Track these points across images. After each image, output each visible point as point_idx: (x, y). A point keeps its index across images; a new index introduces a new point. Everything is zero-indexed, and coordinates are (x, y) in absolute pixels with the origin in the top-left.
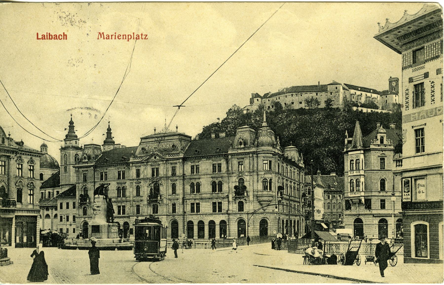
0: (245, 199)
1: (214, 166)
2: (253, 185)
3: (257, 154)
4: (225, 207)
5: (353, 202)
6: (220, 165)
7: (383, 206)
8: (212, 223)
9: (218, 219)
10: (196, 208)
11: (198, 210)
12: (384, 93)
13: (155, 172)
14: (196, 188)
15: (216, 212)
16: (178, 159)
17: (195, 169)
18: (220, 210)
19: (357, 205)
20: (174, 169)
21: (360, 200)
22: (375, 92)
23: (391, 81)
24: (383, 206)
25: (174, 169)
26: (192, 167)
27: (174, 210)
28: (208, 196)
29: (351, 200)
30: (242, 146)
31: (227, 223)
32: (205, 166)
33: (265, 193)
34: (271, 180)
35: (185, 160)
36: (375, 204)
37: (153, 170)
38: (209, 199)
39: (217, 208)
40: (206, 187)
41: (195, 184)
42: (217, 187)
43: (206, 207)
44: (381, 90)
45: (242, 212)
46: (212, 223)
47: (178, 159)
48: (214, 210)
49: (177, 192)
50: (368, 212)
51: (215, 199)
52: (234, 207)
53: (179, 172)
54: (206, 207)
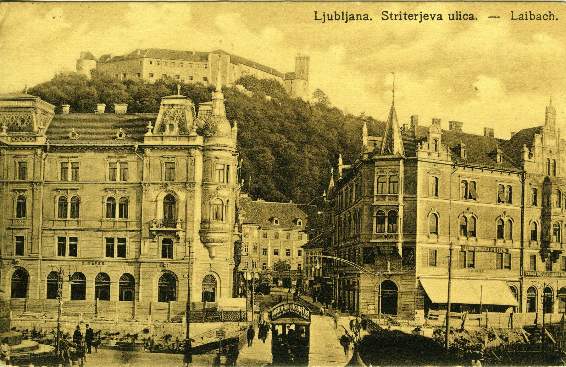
0: (177, 237)
3: (203, 150)
8: (104, 278)
9: (116, 270)
11: (73, 252)
12: (290, 77)
21: (396, 249)
22: (275, 73)
28: (97, 225)
31: (136, 281)
34: (228, 201)
38: (98, 230)
40: (94, 208)
42: (116, 208)
43: (91, 247)
44: (284, 73)
47: (34, 148)
51: (112, 233)
52: (152, 249)
54: (91, 247)
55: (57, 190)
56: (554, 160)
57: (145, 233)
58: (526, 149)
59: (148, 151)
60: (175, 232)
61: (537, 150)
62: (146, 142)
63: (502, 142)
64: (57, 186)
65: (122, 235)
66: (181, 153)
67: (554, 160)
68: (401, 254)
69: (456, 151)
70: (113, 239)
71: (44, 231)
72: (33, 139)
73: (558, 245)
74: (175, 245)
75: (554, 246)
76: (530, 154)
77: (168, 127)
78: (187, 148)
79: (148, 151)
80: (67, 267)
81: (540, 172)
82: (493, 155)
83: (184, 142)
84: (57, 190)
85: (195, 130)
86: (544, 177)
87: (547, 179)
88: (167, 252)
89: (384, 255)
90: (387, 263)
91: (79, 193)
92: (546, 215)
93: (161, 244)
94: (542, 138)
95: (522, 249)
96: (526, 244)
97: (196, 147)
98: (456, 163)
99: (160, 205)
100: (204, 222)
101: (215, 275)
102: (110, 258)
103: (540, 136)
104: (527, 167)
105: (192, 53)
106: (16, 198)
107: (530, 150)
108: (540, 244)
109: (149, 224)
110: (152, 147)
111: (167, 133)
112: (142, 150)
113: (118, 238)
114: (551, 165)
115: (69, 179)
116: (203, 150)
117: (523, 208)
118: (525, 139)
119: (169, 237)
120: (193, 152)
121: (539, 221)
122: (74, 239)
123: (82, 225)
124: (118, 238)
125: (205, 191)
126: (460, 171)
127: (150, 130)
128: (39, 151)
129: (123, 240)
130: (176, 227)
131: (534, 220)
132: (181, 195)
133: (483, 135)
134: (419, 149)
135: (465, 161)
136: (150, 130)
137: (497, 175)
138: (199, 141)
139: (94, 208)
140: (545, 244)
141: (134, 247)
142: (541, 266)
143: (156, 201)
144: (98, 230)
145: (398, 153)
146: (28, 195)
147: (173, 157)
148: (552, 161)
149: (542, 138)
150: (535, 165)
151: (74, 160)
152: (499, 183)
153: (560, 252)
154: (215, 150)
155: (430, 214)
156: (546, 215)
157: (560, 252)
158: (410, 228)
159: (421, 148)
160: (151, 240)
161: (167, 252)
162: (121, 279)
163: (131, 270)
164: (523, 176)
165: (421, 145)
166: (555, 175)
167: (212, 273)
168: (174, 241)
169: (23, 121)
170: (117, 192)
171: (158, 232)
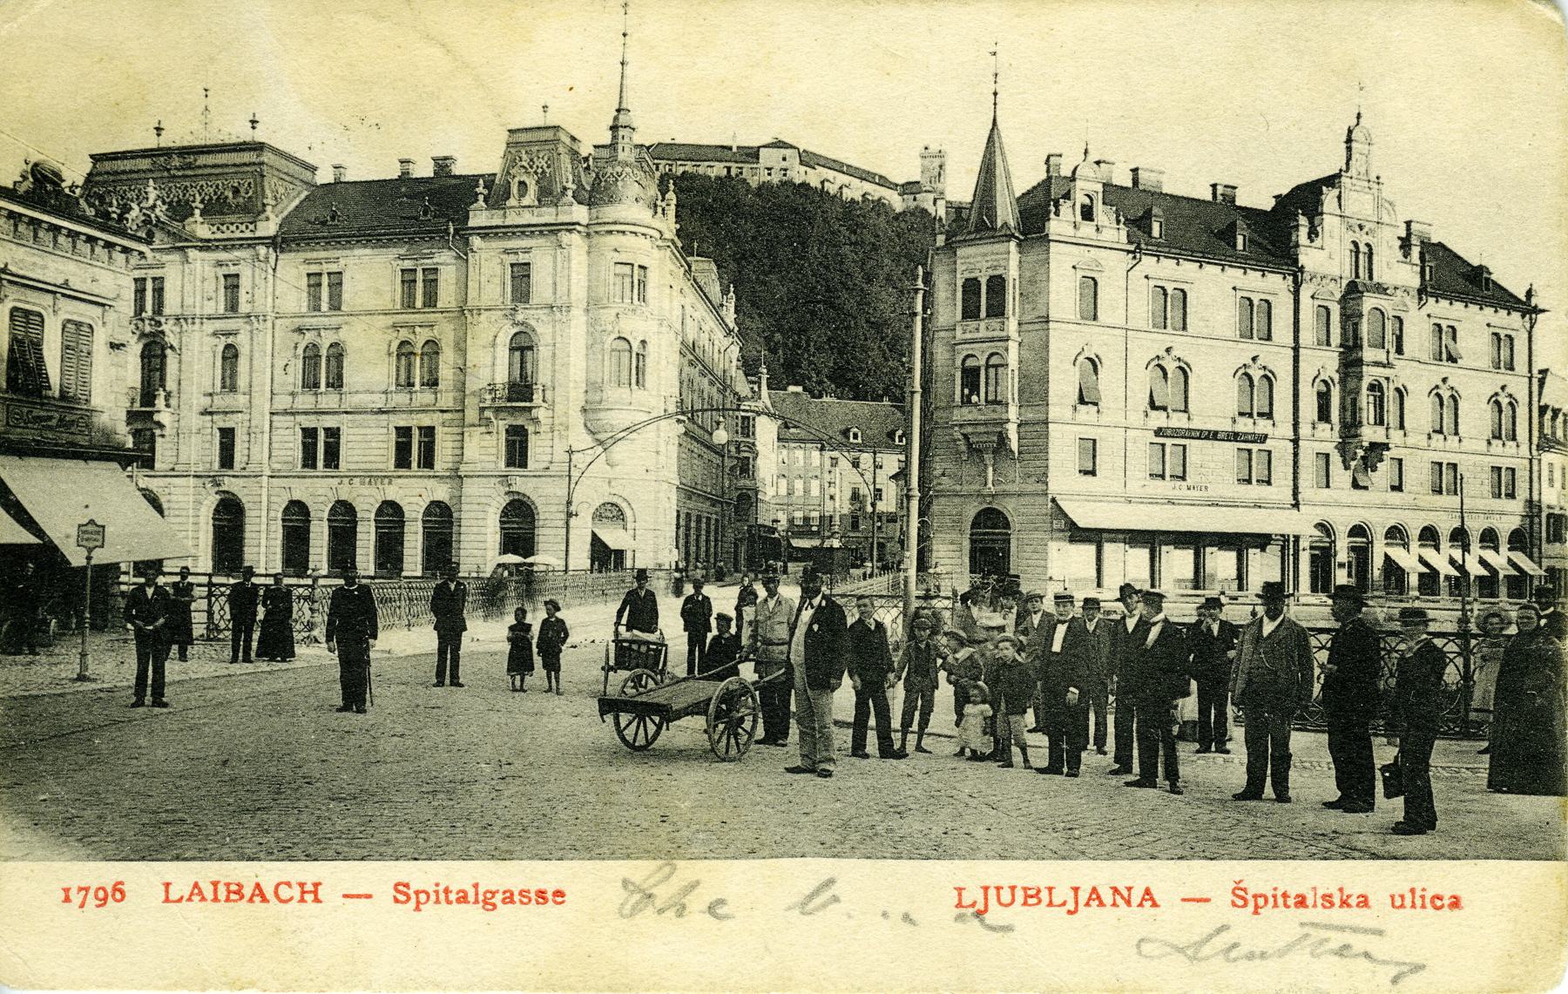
0: (536, 421)
3: (588, 235)
5: (969, 445)
8: (391, 514)
10: (321, 449)
12: (910, 188)
13: (149, 294)
15: (409, 466)
17: (327, 290)
18: (428, 461)
19: (988, 457)
21: (1003, 439)
22: (883, 182)
23: (926, 153)
26: (314, 280)
28: (379, 401)
29: (965, 436)
37: (140, 282)
38: (381, 412)
39: (414, 449)
41: (324, 352)
43: (366, 445)
45: (521, 471)
46: (391, 514)
48: (402, 460)
52: (486, 449)
54: (366, 445)
55: (300, 330)
56: (1368, 245)
57: (472, 415)
58: (1303, 220)
59: (476, 241)
60: (530, 409)
61: (1330, 222)
62: (471, 223)
63: (1249, 213)
64: (298, 322)
65: (426, 421)
66: (541, 241)
67: (1368, 245)
68: (1014, 446)
69: (1139, 224)
70: (410, 429)
71: (275, 418)
72: (251, 227)
73: (1381, 430)
74: (532, 439)
75: (1370, 433)
76: (1313, 233)
77: (515, 189)
78: (553, 229)
79: (476, 241)
80: (319, 493)
81: (1337, 273)
82: (1228, 235)
83: (547, 215)
84: (300, 330)
85: (570, 193)
86: (1345, 282)
87: (1353, 291)
88: (517, 452)
89: (979, 451)
90: (985, 471)
91: (343, 335)
92: (1351, 363)
93: (503, 436)
94: (1339, 198)
95: (1296, 442)
96: (1305, 430)
97: (570, 227)
98: (1138, 247)
99: (503, 353)
100: (593, 387)
101: (624, 505)
102: (402, 472)
103: (1336, 192)
104: (1308, 258)
105: (730, 148)
106: (221, 348)
107: (1311, 222)
108: (1337, 428)
109: (478, 394)
110: (486, 232)
111: (512, 202)
112: (463, 235)
113: (420, 428)
114: (1361, 256)
115: (325, 306)
116: (588, 235)
117: (1296, 349)
118: (1305, 200)
119: (519, 422)
120: (565, 237)
121: (1336, 377)
122: (333, 433)
123: (351, 401)
124: (420, 428)
125: (593, 323)
126: (1148, 262)
127: (481, 198)
128: (262, 250)
129: (429, 432)
130: (531, 400)
131: (1322, 377)
132: (544, 331)
133: (1209, 197)
134: (1052, 216)
135: (1158, 245)
136: (481, 198)
137: (1234, 275)
138: (580, 213)
140: (1350, 427)
141: (451, 445)
142: (1341, 477)
143: (494, 345)
144: (381, 412)
145: (1005, 224)
146: (242, 341)
147: (527, 250)
148: (1363, 248)
149: (1339, 198)
150: (1325, 256)
151: (334, 268)
152: (1240, 294)
153: (1386, 447)
154: (610, 232)
155: (1081, 358)
156: (1351, 363)
157: (1386, 447)
158: (1035, 389)
159: (1057, 214)
160: (483, 429)
161: (517, 452)
162: (425, 514)
163: (442, 493)
164: (1295, 278)
165: (1057, 205)
166: (1371, 278)
167: (615, 500)
168: (531, 429)
169: (236, 191)
170: (418, 329)
171: (498, 410)
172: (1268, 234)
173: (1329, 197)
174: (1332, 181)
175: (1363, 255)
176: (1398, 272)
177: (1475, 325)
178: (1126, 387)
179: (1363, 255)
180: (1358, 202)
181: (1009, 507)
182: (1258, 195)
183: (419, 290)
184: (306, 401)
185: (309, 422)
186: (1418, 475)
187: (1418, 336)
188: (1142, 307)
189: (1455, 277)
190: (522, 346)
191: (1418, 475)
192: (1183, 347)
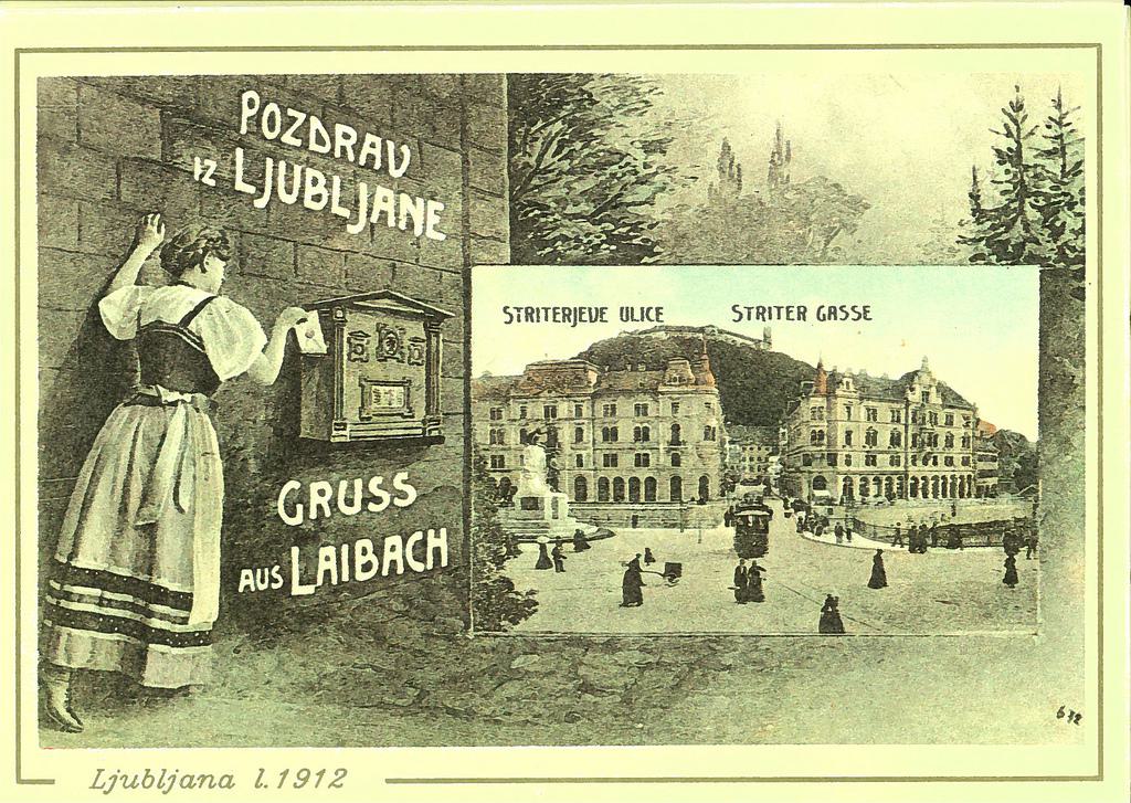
1: (637, 407)
2: (692, 434)
4: (652, 460)
6: (645, 407)
7: (848, 463)
8: (635, 480)
10: (611, 460)
13: (551, 412)
14: (611, 435)
16: (585, 395)
20: (578, 408)
24: (848, 463)
25: (578, 408)
26: (606, 407)
27: (580, 464)
30: (677, 383)
32: (625, 407)
33: (708, 442)
35: (594, 396)
36: (841, 459)
39: (642, 461)
40: (626, 433)
42: (642, 435)
43: (626, 460)
48: (637, 465)
49: (585, 440)
50: (831, 468)
52: (666, 460)
53: (586, 412)
54: (626, 460)
80: (612, 474)
88: (676, 462)
104: (910, 397)
139: (626, 433)
142: (919, 463)
150: (915, 397)
161: (676, 462)
172: (898, 390)
173: (916, 378)
174: (916, 373)
175: (926, 395)
176: (935, 399)
177: (958, 416)
178: (859, 438)
179: (926, 395)
180: (925, 379)
181: (824, 475)
182: (896, 376)
183: (641, 410)
184: (606, 445)
185: (608, 452)
186: (941, 460)
187: (942, 420)
188: (863, 414)
189: (952, 399)
190: (676, 428)
191: (941, 460)
192: (876, 427)
